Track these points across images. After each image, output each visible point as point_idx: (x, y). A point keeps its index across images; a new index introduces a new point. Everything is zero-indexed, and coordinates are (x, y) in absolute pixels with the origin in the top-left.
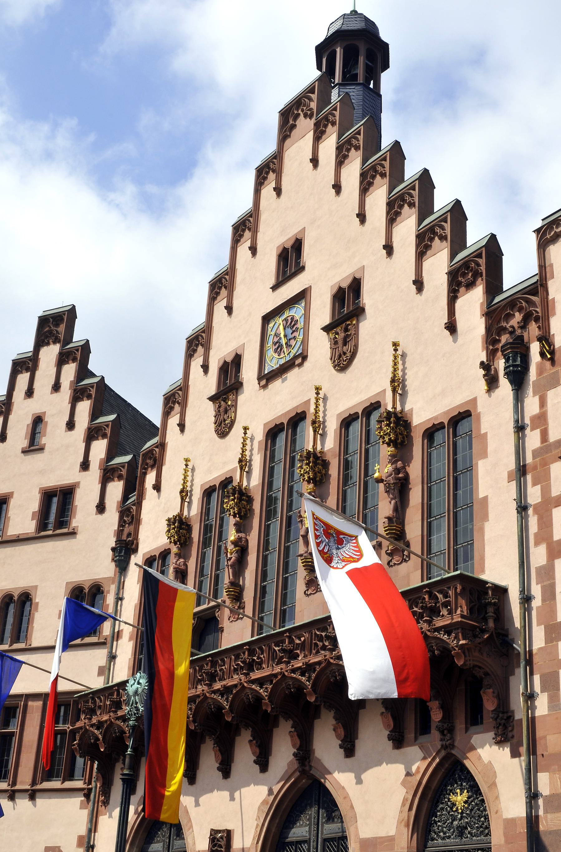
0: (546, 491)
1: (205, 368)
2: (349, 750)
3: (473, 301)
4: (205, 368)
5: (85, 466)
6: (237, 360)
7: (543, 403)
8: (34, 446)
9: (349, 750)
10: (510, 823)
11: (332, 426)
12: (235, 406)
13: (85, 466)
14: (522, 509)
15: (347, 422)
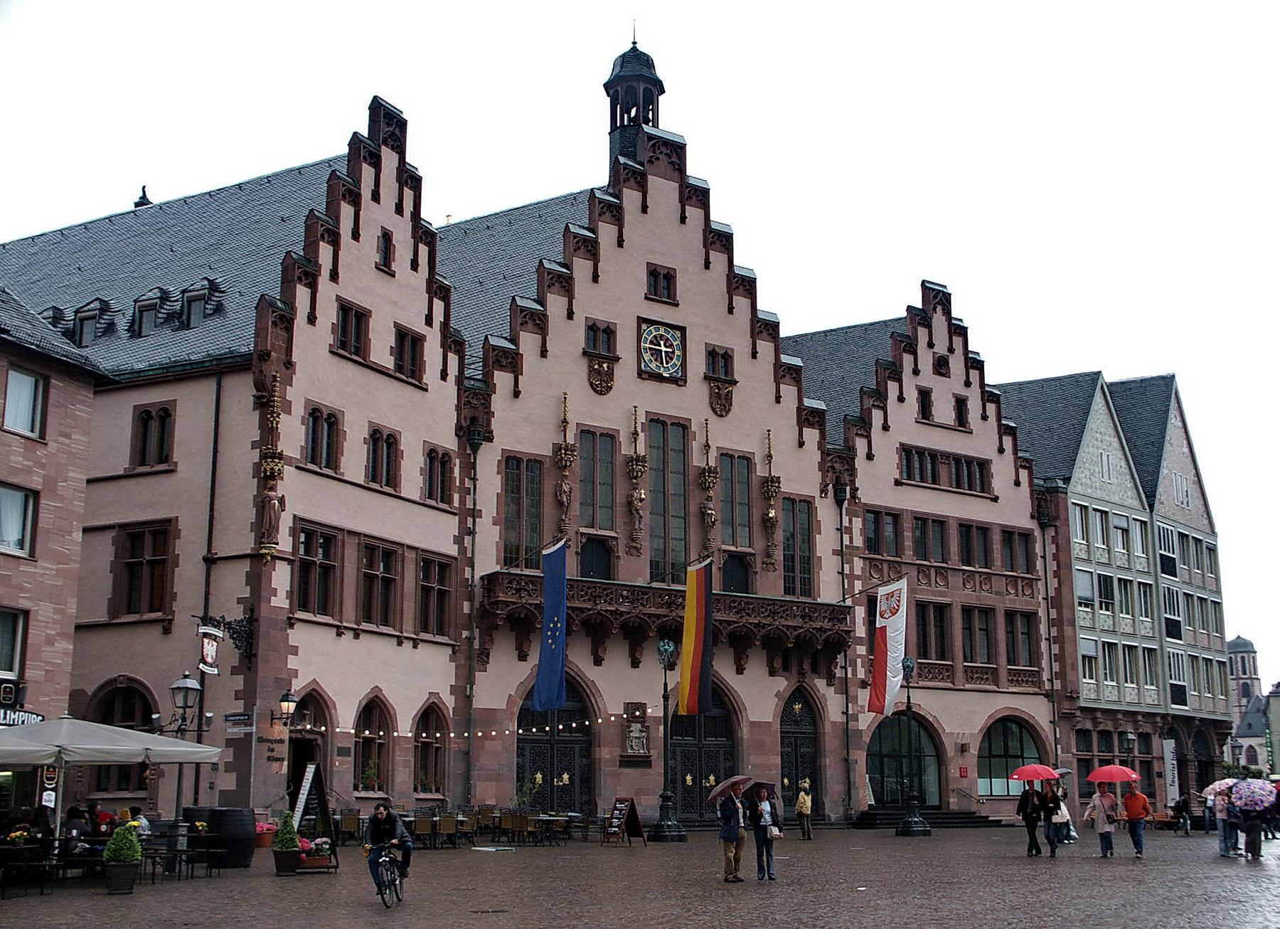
0: (852, 569)
1: (570, 315)
2: (740, 670)
3: (812, 435)
4: (570, 315)
5: (429, 321)
6: (610, 332)
7: (850, 522)
8: (385, 266)
9: (740, 670)
10: (834, 723)
11: (713, 453)
12: (610, 374)
13: (429, 321)
14: (841, 573)
15: (726, 455)
